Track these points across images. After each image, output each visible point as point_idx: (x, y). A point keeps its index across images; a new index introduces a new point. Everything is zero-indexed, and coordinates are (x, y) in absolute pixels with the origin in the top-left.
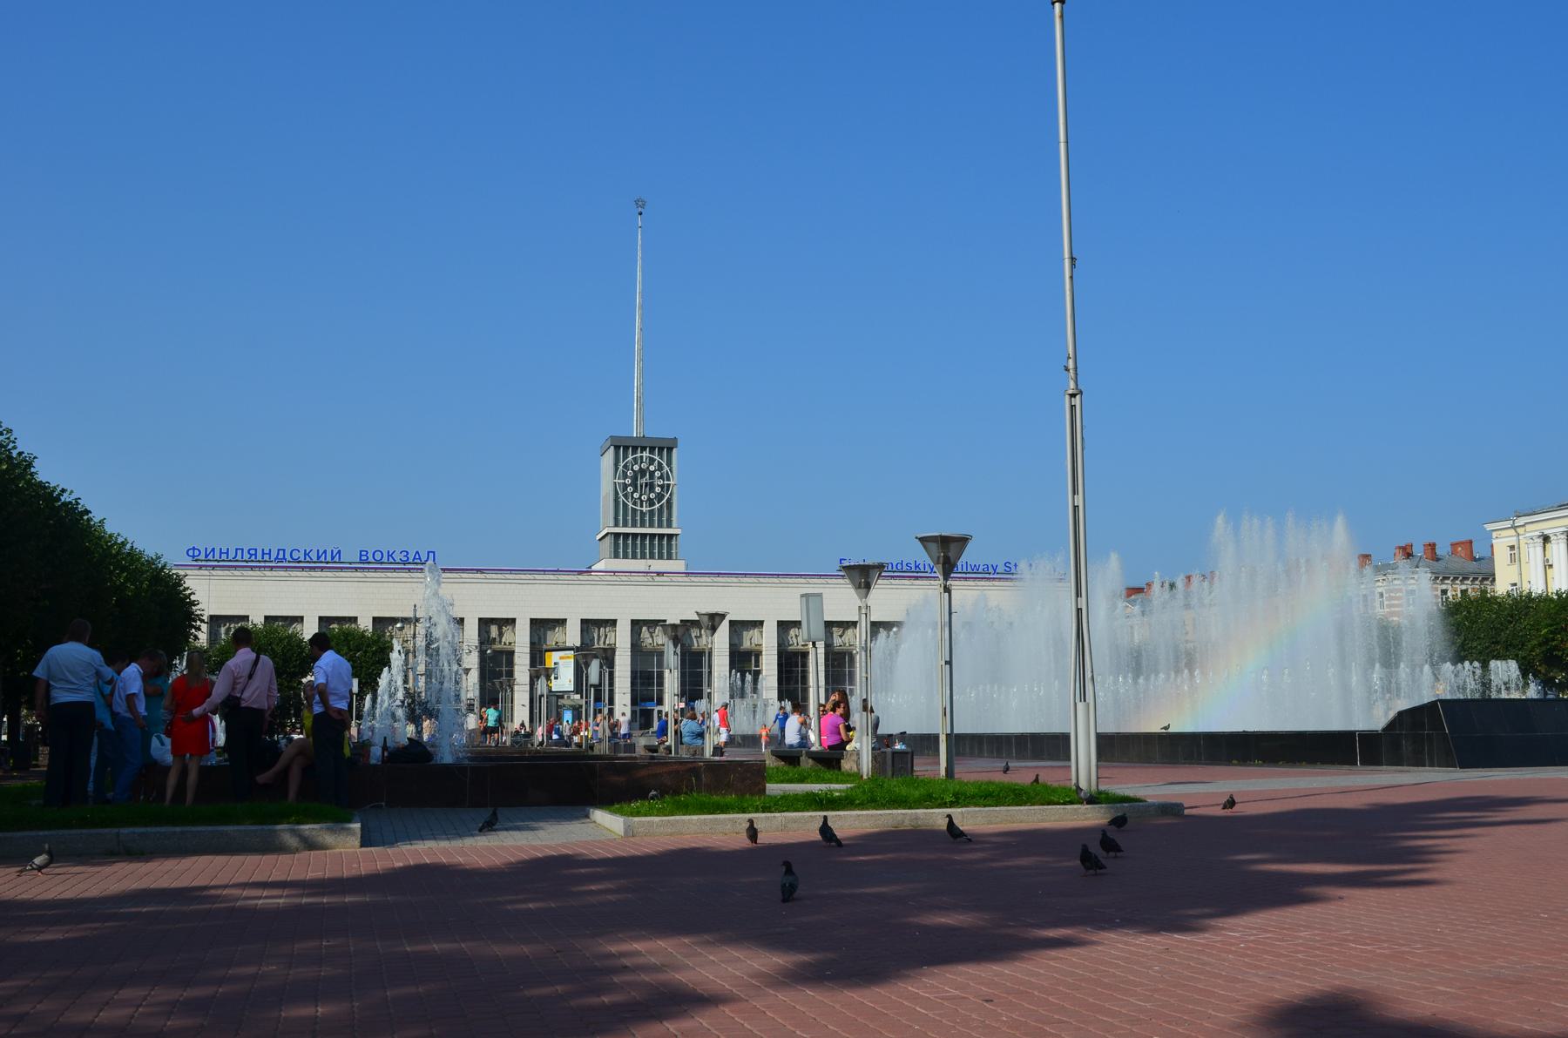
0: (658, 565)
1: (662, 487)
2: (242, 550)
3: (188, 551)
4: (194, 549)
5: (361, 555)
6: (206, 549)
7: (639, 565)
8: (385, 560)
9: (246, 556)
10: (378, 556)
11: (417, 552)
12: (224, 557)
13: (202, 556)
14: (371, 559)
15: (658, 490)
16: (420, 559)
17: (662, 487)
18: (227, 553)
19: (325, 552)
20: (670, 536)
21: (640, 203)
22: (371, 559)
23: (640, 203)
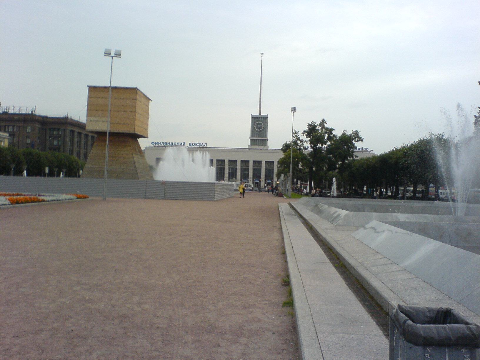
0: (262, 147)
1: (264, 127)
2: (163, 143)
3: (152, 143)
4: (153, 142)
5: (190, 144)
6: (156, 142)
7: (256, 147)
8: (195, 145)
9: (164, 144)
10: (193, 144)
11: (203, 144)
12: (159, 144)
13: (155, 144)
14: (192, 145)
15: (262, 128)
16: (203, 145)
17: (264, 127)
18: (160, 143)
19: (182, 144)
20: (265, 140)
21: (262, 54)
22: (192, 145)
23: (262, 54)
